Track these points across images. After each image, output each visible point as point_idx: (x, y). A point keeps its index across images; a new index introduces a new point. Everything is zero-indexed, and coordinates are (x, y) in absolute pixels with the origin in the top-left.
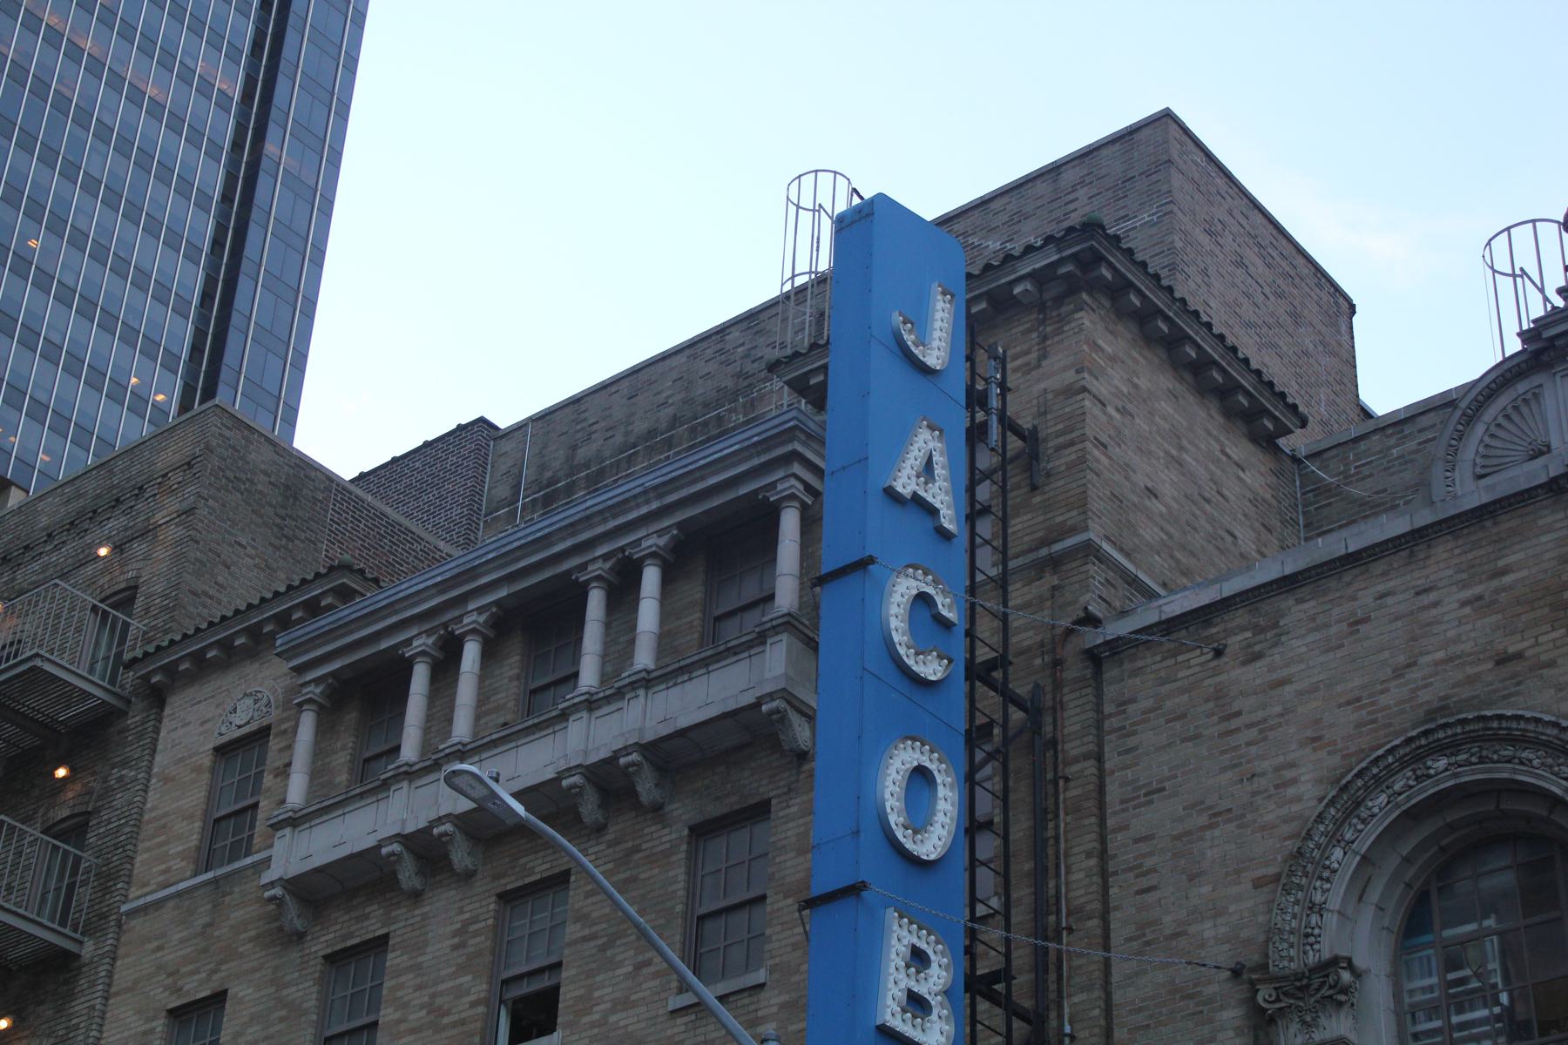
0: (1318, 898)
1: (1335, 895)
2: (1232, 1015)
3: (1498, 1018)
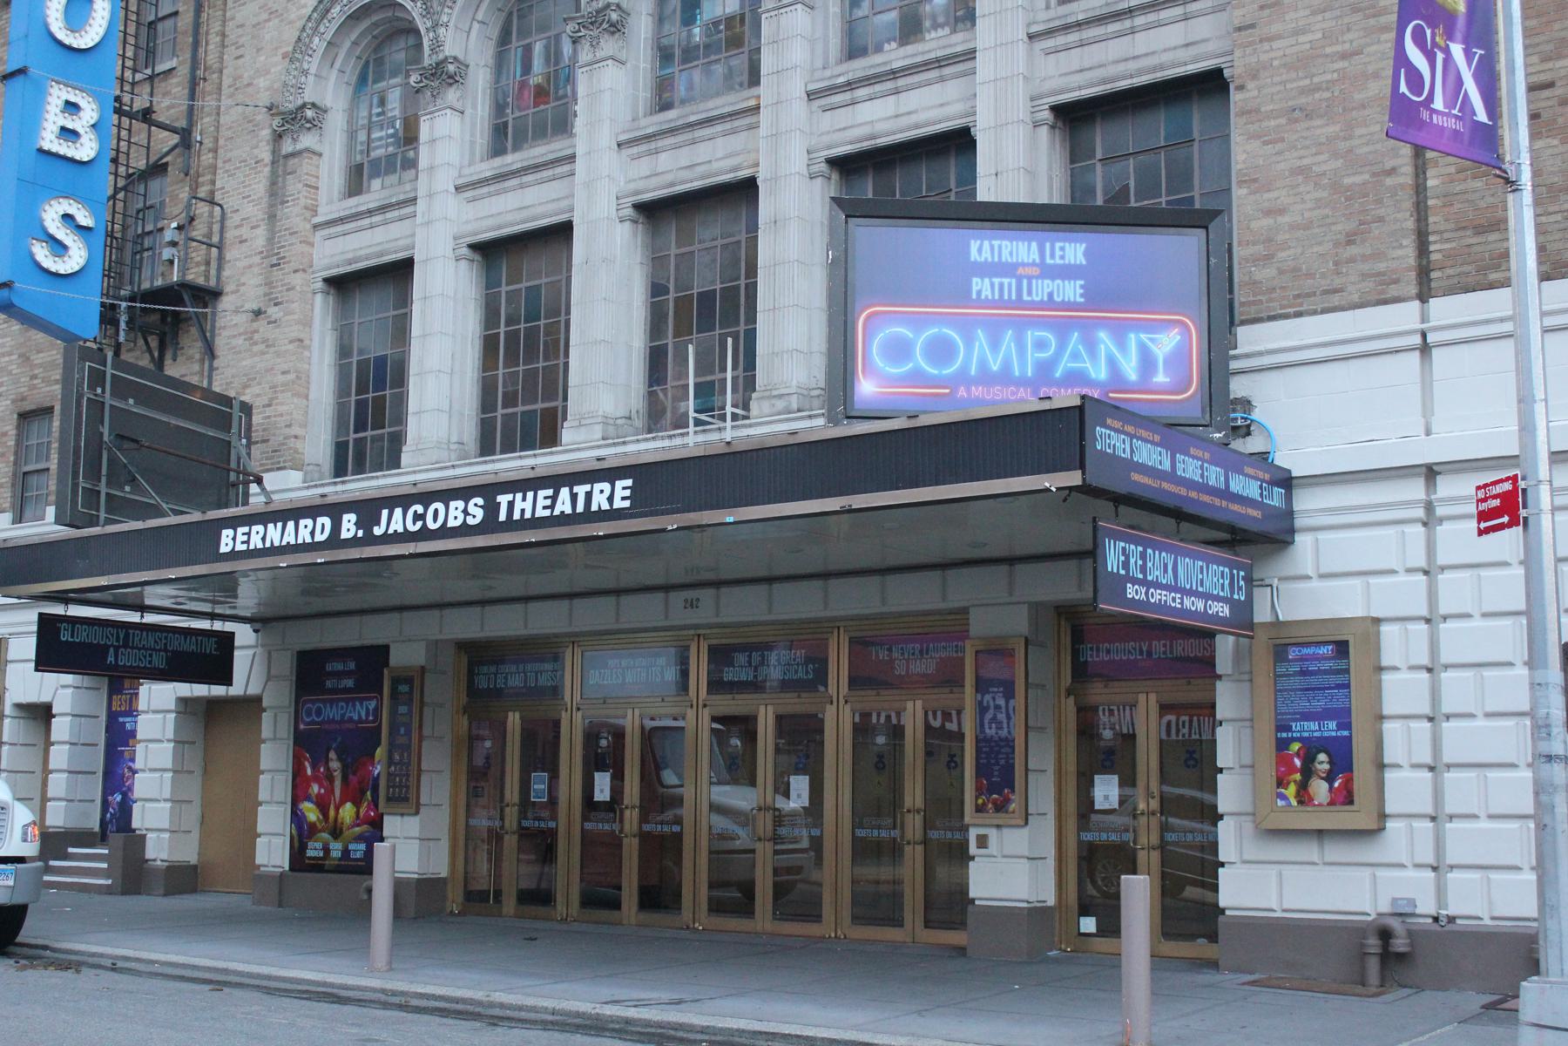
0: (306, 66)
1: (313, 65)
2: (266, 133)
3: (392, 136)
